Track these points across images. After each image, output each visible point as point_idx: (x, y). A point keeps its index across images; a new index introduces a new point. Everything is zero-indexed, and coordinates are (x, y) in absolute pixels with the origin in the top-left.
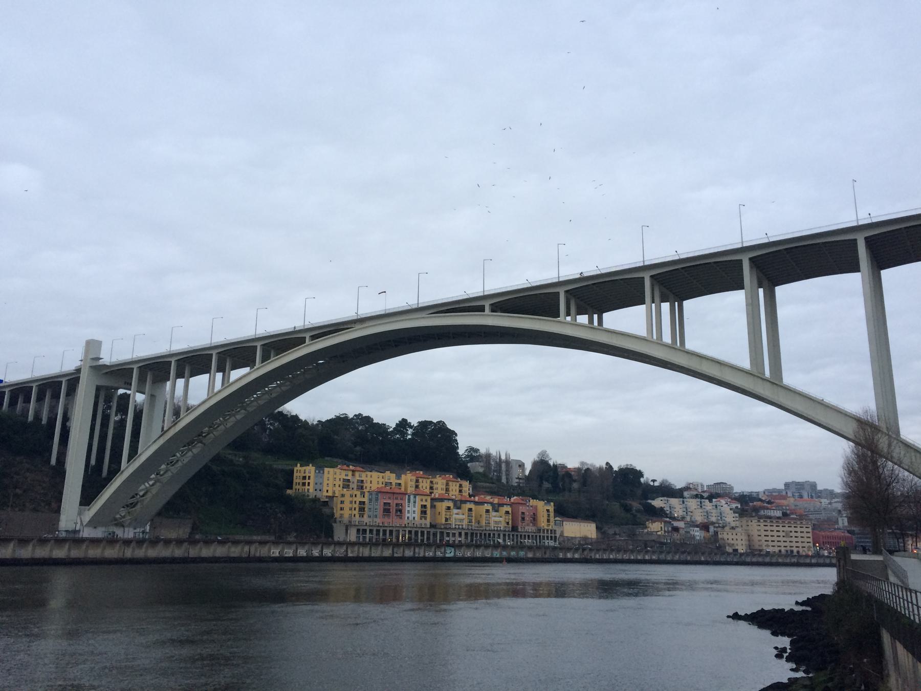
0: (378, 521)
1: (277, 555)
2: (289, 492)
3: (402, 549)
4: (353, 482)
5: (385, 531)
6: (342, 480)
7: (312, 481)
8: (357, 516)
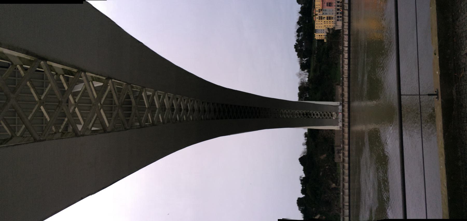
0: (333, 8)
1: (347, 66)
2: (325, 41)
3: (345, 4)
4: (320, 14)
5: (338, 6)
6: (319, 20)
7: (321, 34)
8: (333, 20)
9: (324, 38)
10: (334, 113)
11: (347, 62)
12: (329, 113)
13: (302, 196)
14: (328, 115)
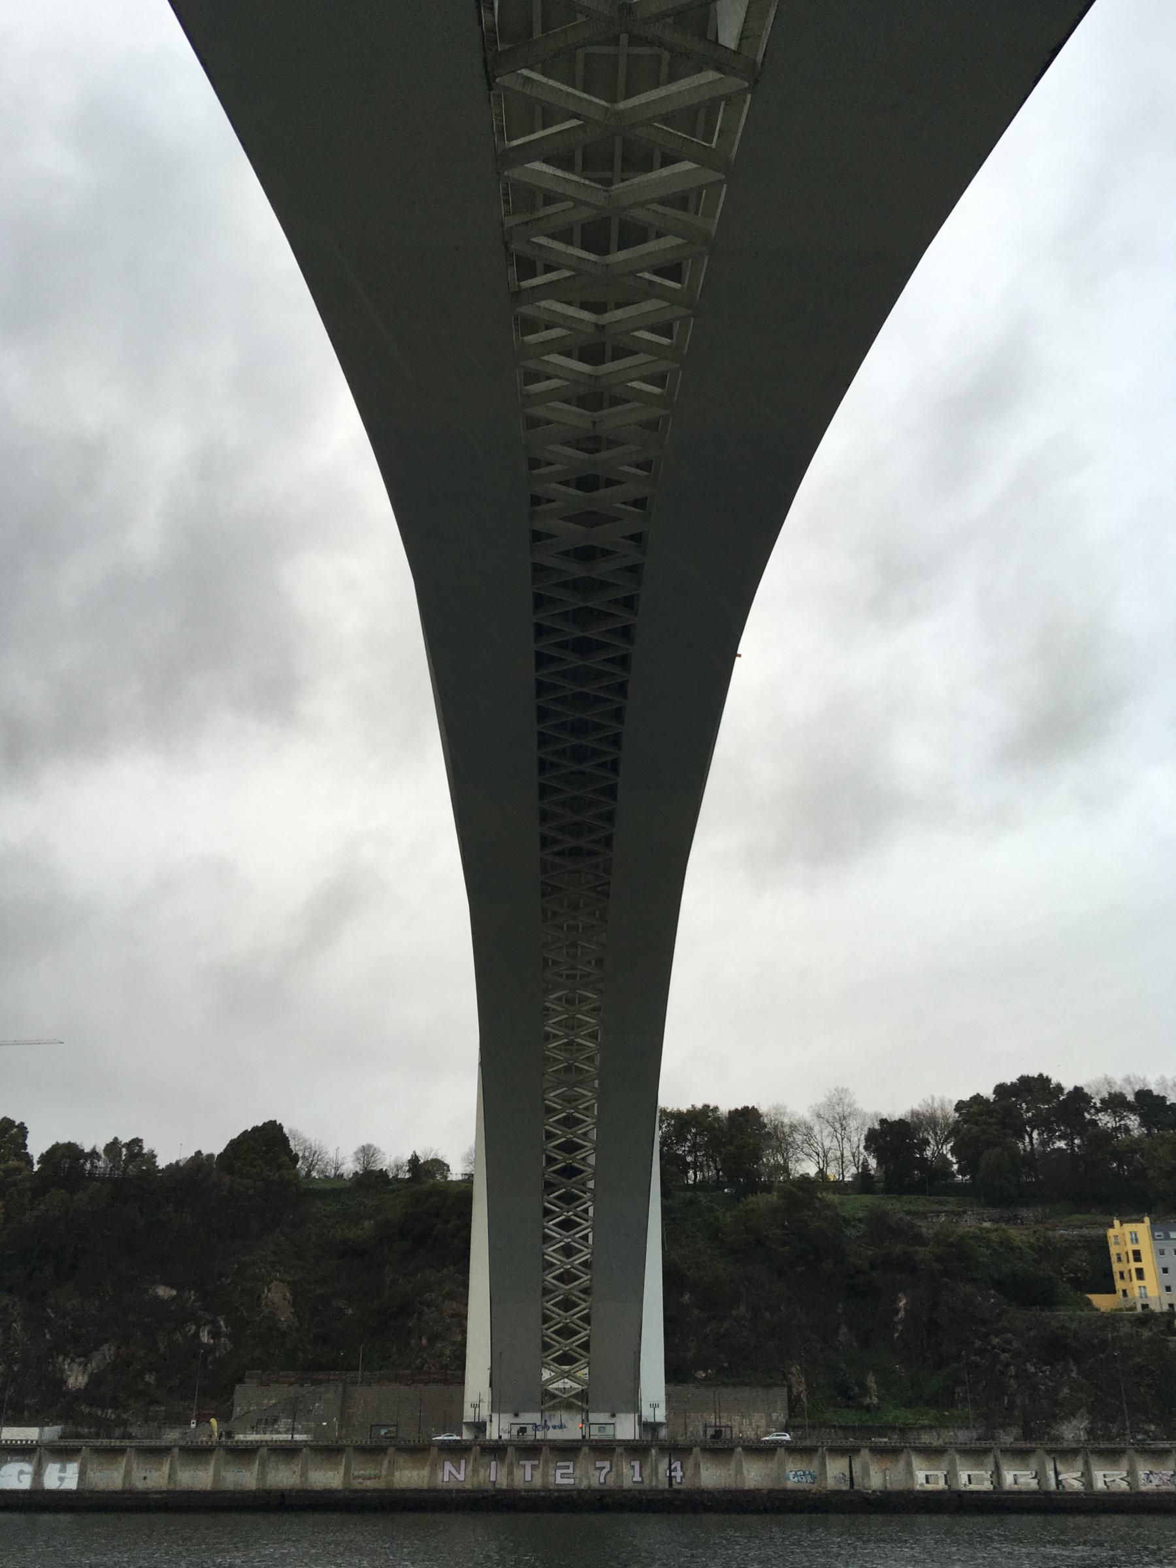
2: (1102, 1302)
7: (1148, 1263)
9: (1124, 1292)
10: (584, 1373)
11: (973, 1487)
12: (582, 1336)
13: (37, 1146)
14: (566, 1332)
